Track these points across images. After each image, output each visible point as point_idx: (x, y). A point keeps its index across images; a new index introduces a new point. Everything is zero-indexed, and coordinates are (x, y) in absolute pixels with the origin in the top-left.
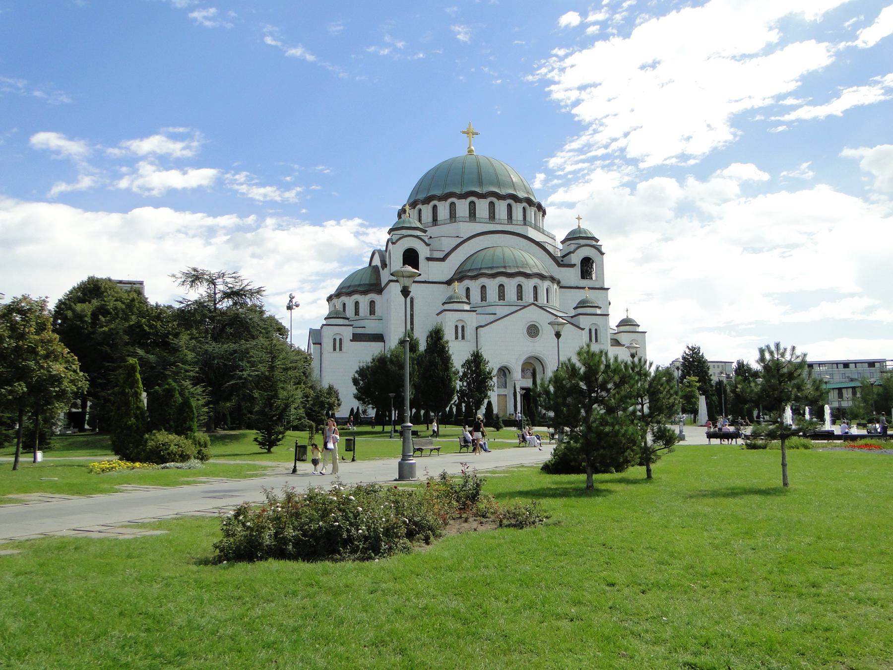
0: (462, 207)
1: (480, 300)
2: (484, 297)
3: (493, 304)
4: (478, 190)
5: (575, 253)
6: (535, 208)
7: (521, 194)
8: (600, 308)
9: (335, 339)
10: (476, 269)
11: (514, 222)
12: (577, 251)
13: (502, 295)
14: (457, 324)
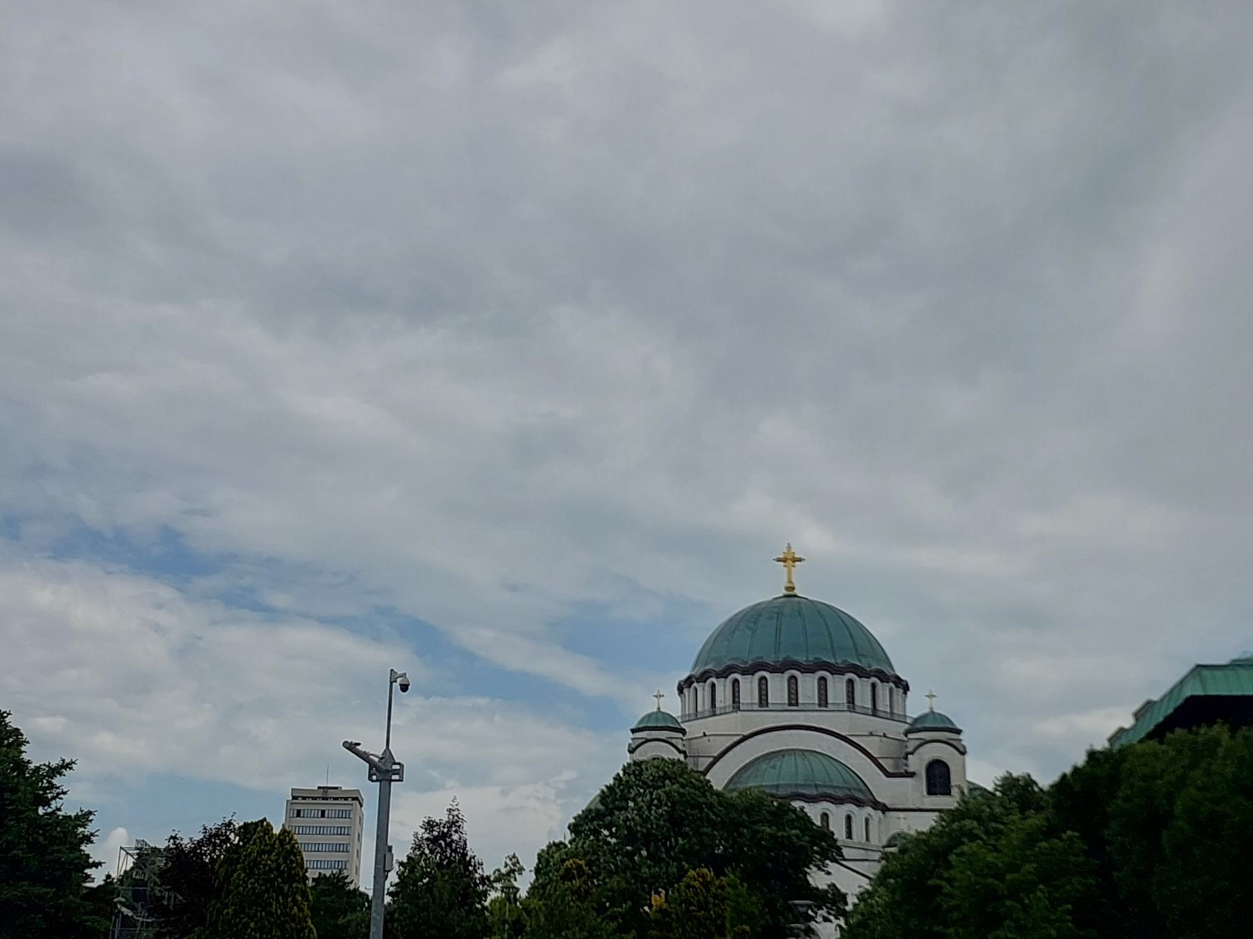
0: (749, 686)
5: (916, 754)
6: (874, 679)
11: (830, 707)
12: (921, 750)
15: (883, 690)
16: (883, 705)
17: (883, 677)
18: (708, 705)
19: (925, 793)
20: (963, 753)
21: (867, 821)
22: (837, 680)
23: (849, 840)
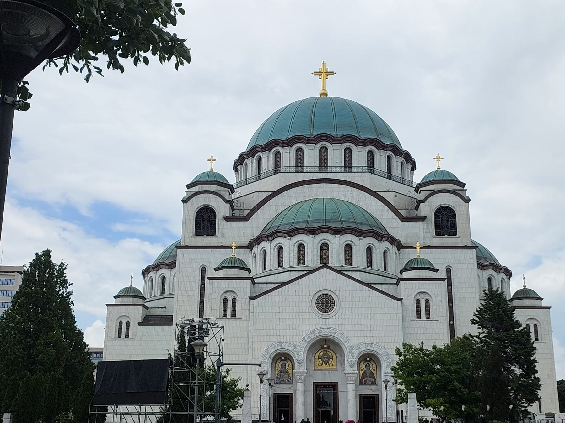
1: (276, 265)
2: (280, 263)
3: (290, 269)
4: (307, 134)
6: (389, 153)
7: (363, 136)
8: (436, 270)
9: (121, 323)
10: (275, 227)
13: (301, 259)
14: (225, 295)
15: (397, 162)
16: (396, 171)
17: (396, 150)
18: (255, 173)
19: (435, 235)
20: (467, 200)
21: (385, 253)
22: (359, 148)
23: (370, 268)
